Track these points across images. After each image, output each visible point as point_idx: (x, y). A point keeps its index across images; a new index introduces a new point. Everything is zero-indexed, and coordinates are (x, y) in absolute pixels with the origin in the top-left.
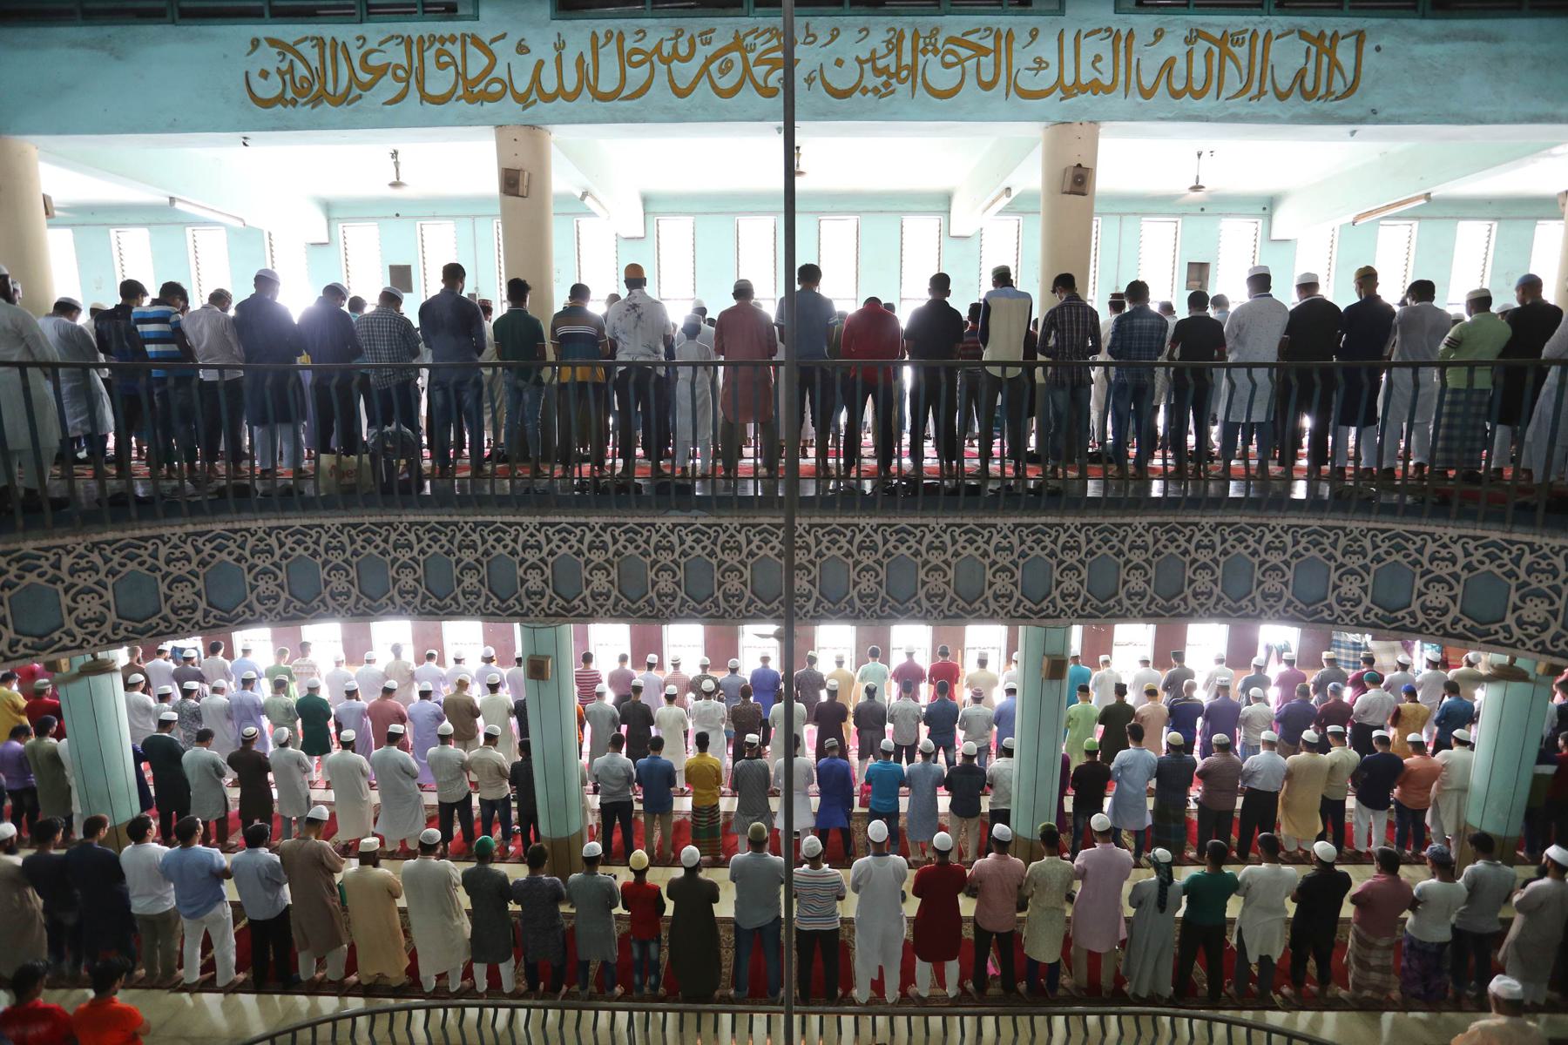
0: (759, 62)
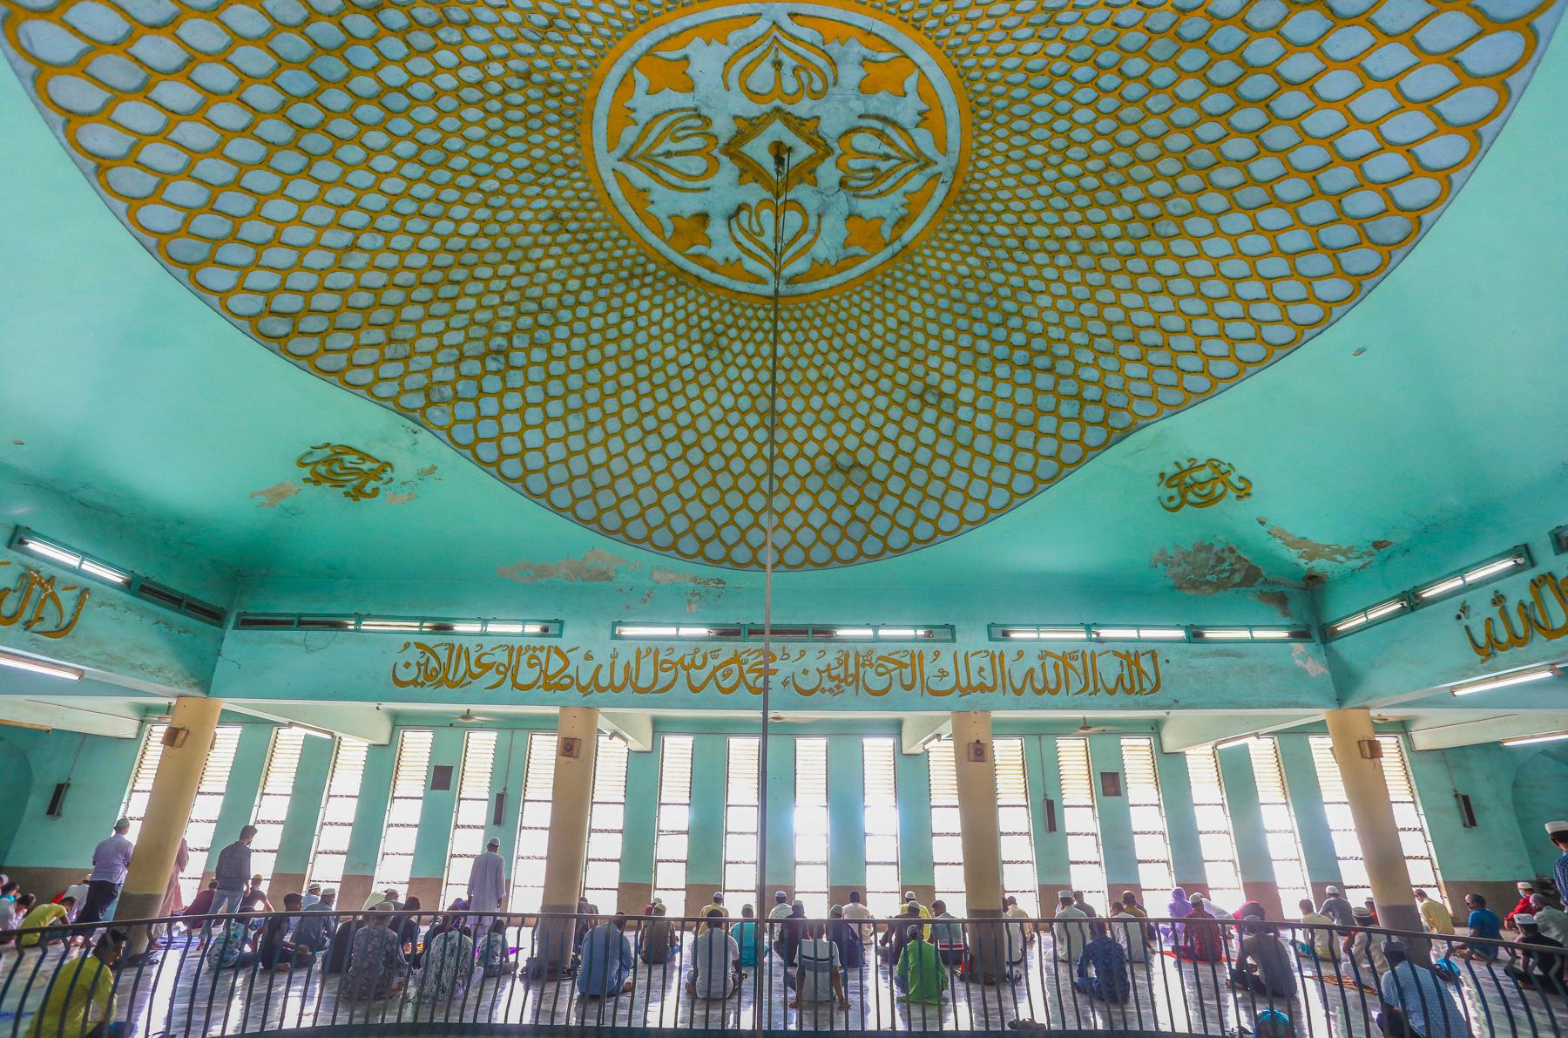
0: (750, 671)
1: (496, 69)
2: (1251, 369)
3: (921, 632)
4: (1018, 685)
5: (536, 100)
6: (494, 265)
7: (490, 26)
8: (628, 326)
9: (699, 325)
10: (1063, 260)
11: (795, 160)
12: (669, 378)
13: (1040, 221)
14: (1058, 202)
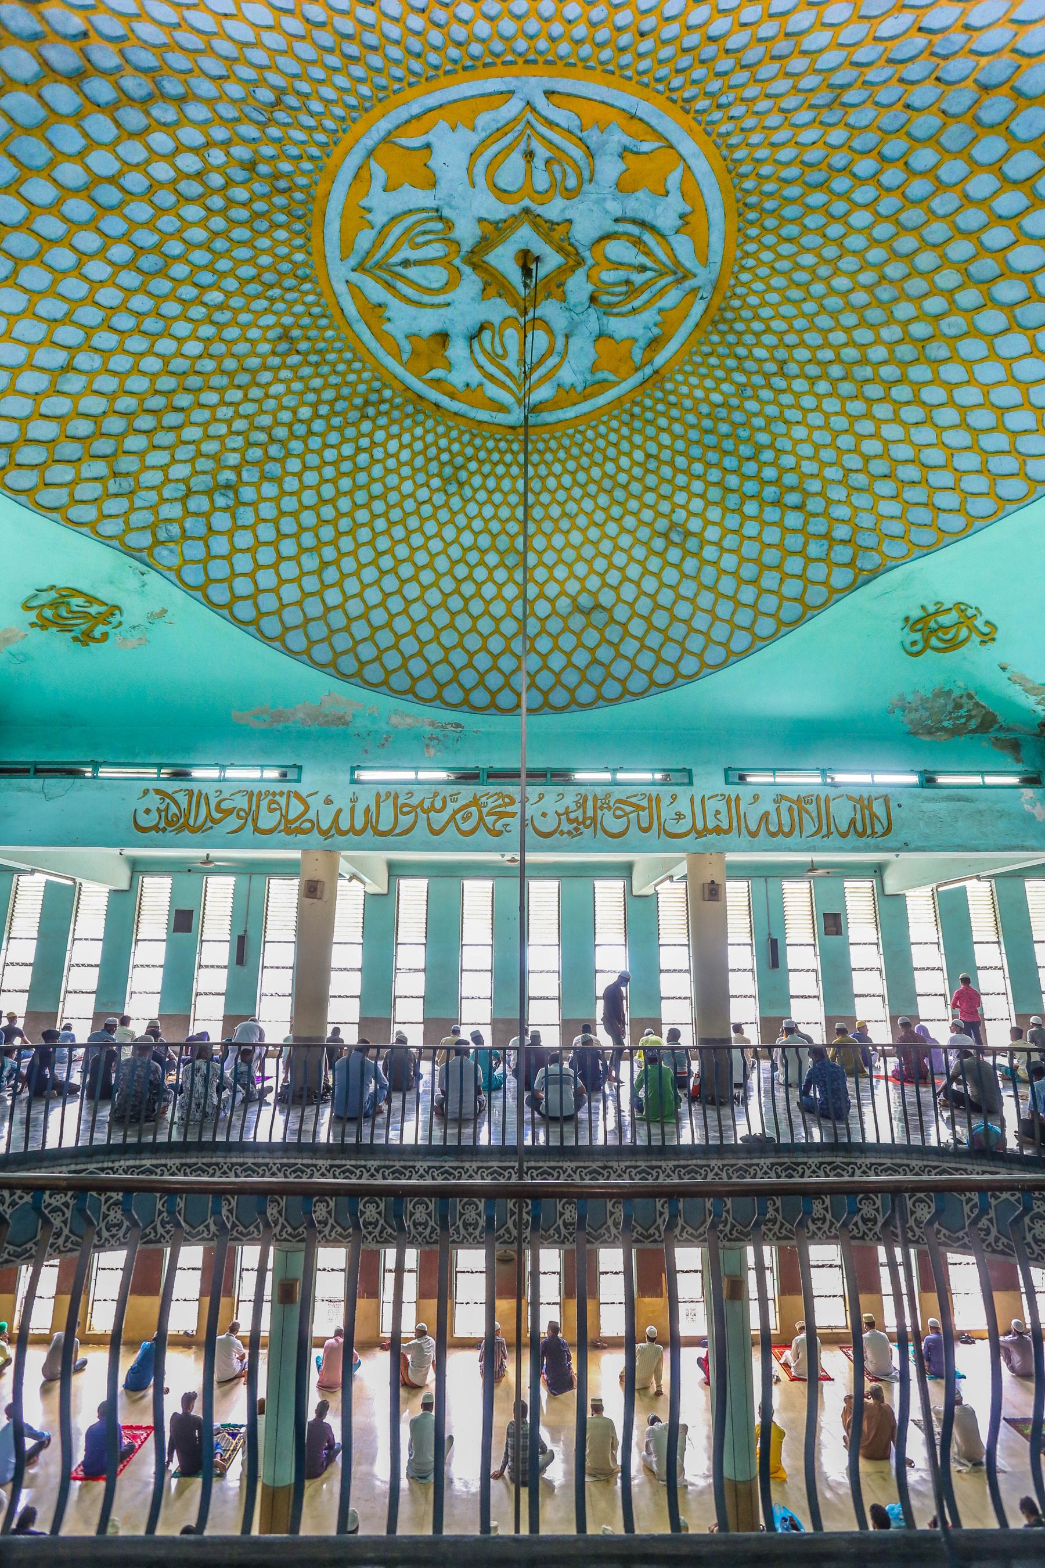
0: (489, 814)
1: (217, 157)
2: (1010, 507)
3: (658, 776)
4: (753, 827)
5: (263, 196)
6: (221, 390)
7: (210, 102)
8: (363, 459)
9: (437, 458)
10: (822, 387)
11: (543, 270)
12: (407, 515)
13: (802, 343)
14: (824, 321)
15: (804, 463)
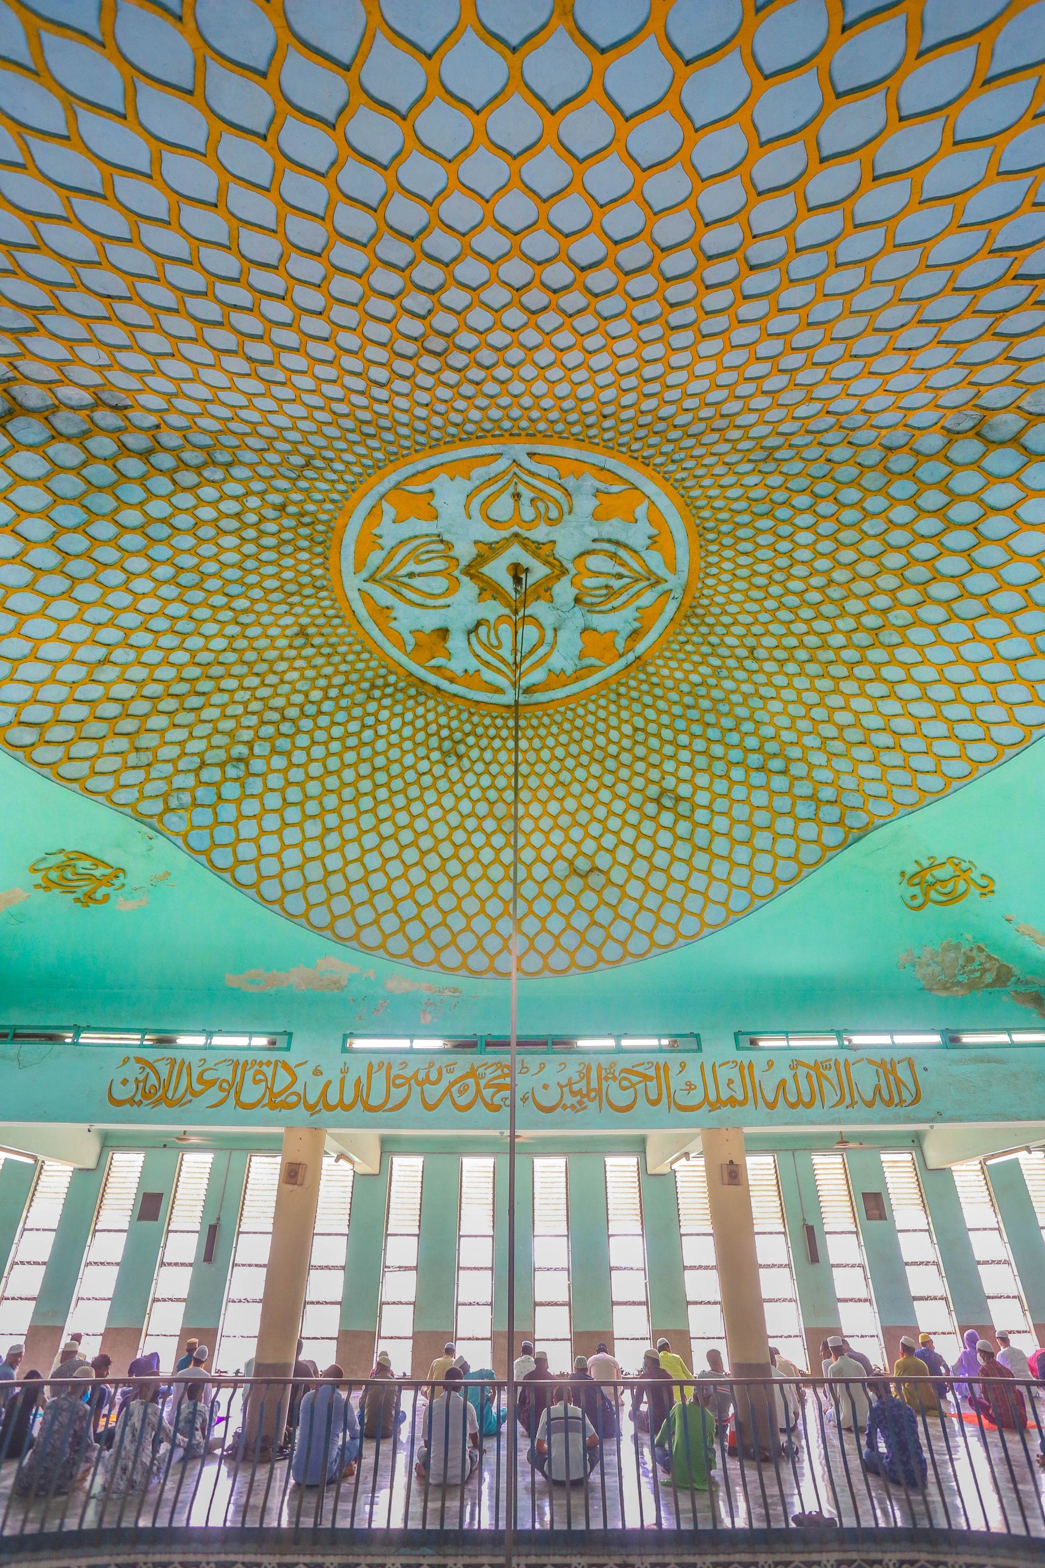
1: (253, 502)
2: (983, 768)
3: (665, 1042)
4: (770, 1098)
5: (290, 529)
6: (240, 677)
8: (368, 735)
9: (437, 733)
10: (791, 668)
11: (532, 579)
14: (784, 615)
15: (783, 733)
